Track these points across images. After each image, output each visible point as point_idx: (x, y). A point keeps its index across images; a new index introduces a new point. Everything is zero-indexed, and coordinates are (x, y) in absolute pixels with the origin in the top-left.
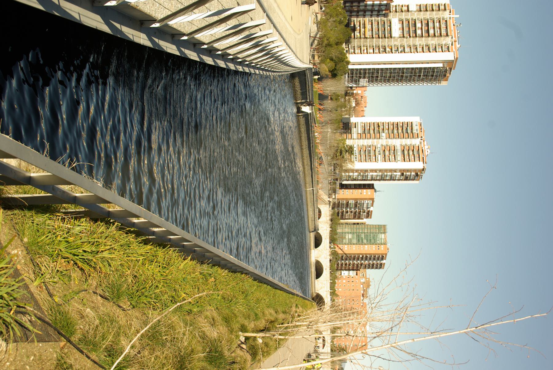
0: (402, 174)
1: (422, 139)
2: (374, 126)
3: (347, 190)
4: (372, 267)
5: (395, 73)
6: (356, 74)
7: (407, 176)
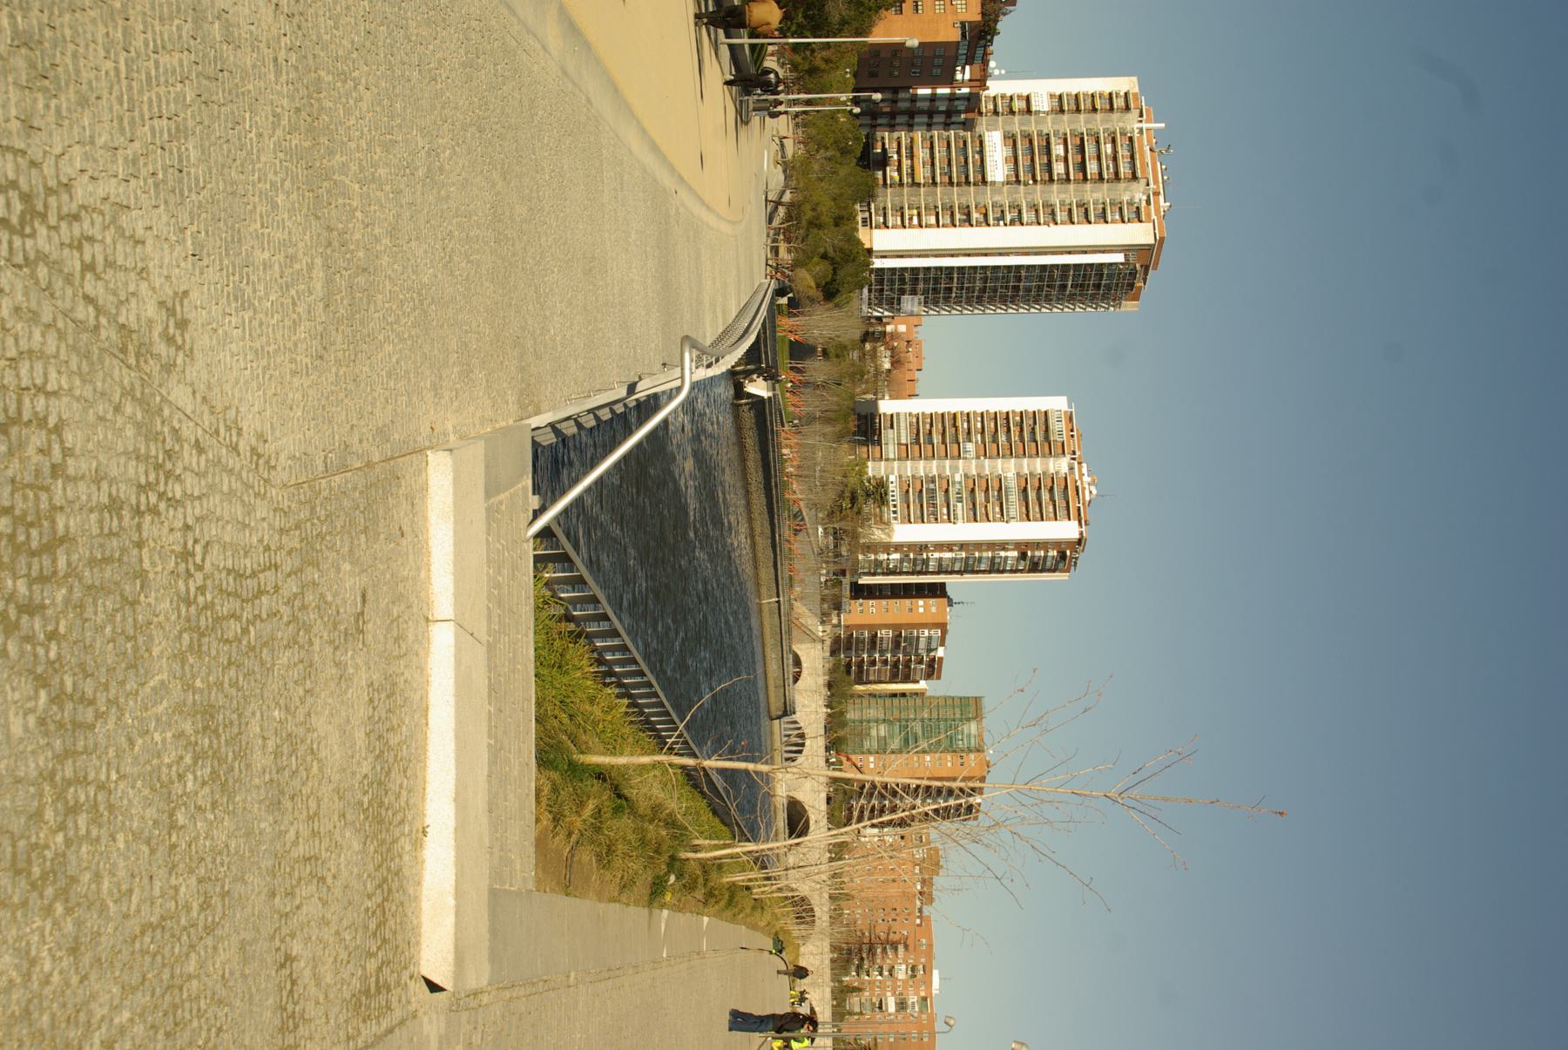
0: (1023, 556)
1: (1074, 459)
3: (871, 602)
5: (997, 279)
6: (892, 282)
7: (1036, 560)
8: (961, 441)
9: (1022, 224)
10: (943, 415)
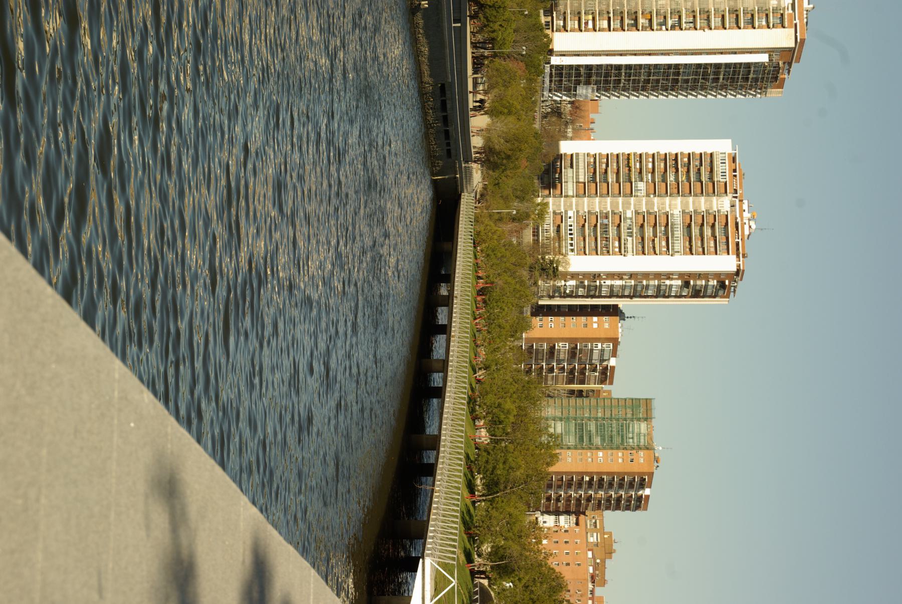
0: (686, 284)
1: (736, 197)
2: (618, 162)
4: (617, 505)
7: (698, 288)
8: (633, 180)
9: (682, 29)
10: (618, 155)
